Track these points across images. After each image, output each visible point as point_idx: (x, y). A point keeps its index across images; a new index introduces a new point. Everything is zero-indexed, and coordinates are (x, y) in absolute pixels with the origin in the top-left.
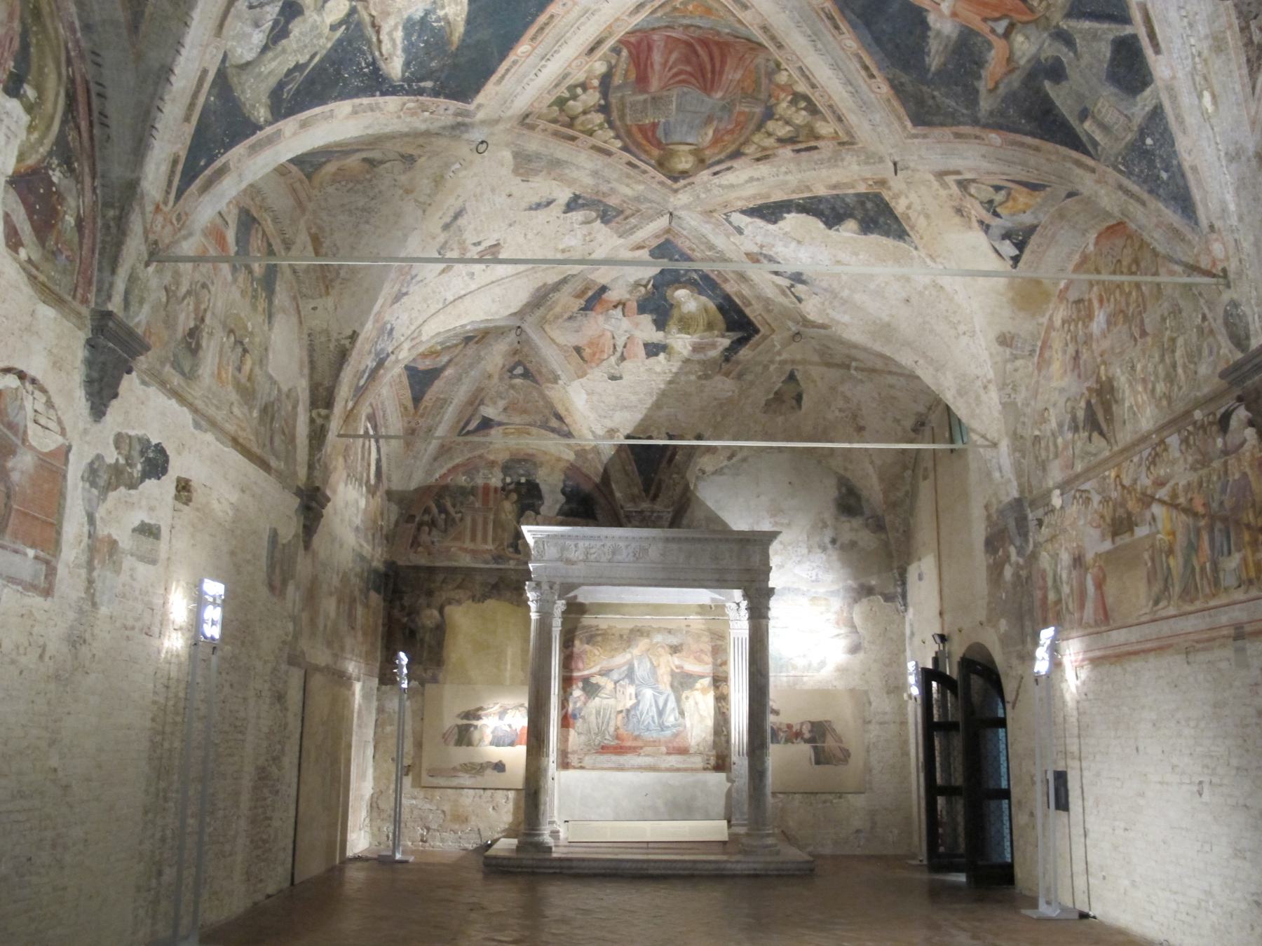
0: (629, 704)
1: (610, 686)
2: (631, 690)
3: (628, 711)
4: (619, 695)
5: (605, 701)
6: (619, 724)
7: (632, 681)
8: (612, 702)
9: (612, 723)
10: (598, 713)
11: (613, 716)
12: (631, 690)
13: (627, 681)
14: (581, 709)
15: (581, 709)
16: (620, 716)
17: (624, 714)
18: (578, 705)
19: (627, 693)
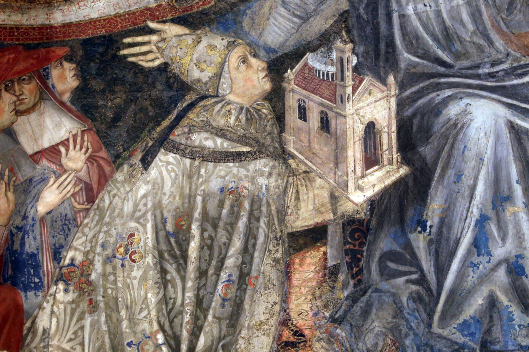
0: (364, 188)
1: (246, 81)
2: (374, 106)
3: (358, 231)
4: (299, 135)
5: (217, 177)
6: (302, 308)
7: (378, 58)
8: (259, 176)
9: (261, 308)
10: (172, 246)
11: (265, 266)
12: (374, 106)
13: (345, 51)
14: (65, 224)
15: (65, 224)
16: (308, 268)
17: (331, 251)
18: (50, 198)
19: (354, 129)
